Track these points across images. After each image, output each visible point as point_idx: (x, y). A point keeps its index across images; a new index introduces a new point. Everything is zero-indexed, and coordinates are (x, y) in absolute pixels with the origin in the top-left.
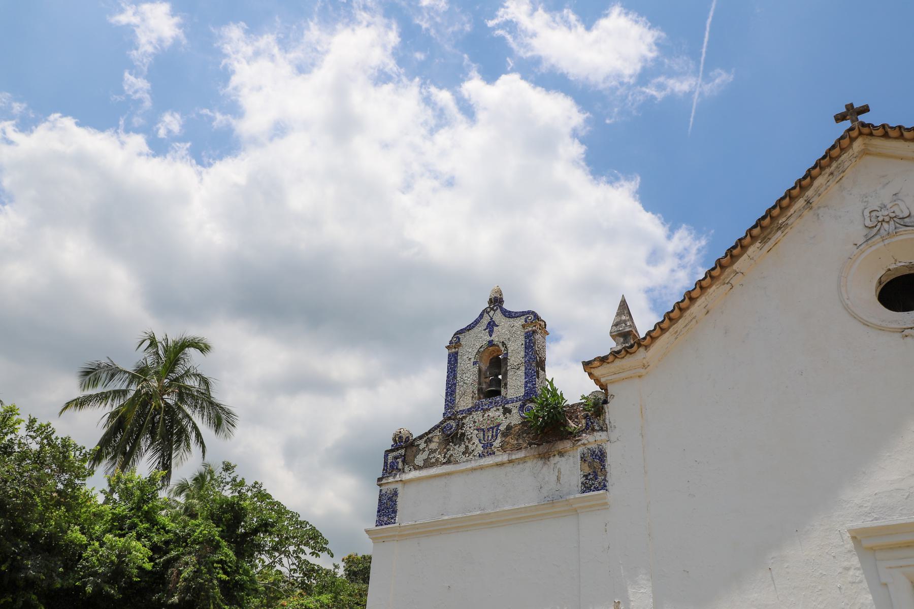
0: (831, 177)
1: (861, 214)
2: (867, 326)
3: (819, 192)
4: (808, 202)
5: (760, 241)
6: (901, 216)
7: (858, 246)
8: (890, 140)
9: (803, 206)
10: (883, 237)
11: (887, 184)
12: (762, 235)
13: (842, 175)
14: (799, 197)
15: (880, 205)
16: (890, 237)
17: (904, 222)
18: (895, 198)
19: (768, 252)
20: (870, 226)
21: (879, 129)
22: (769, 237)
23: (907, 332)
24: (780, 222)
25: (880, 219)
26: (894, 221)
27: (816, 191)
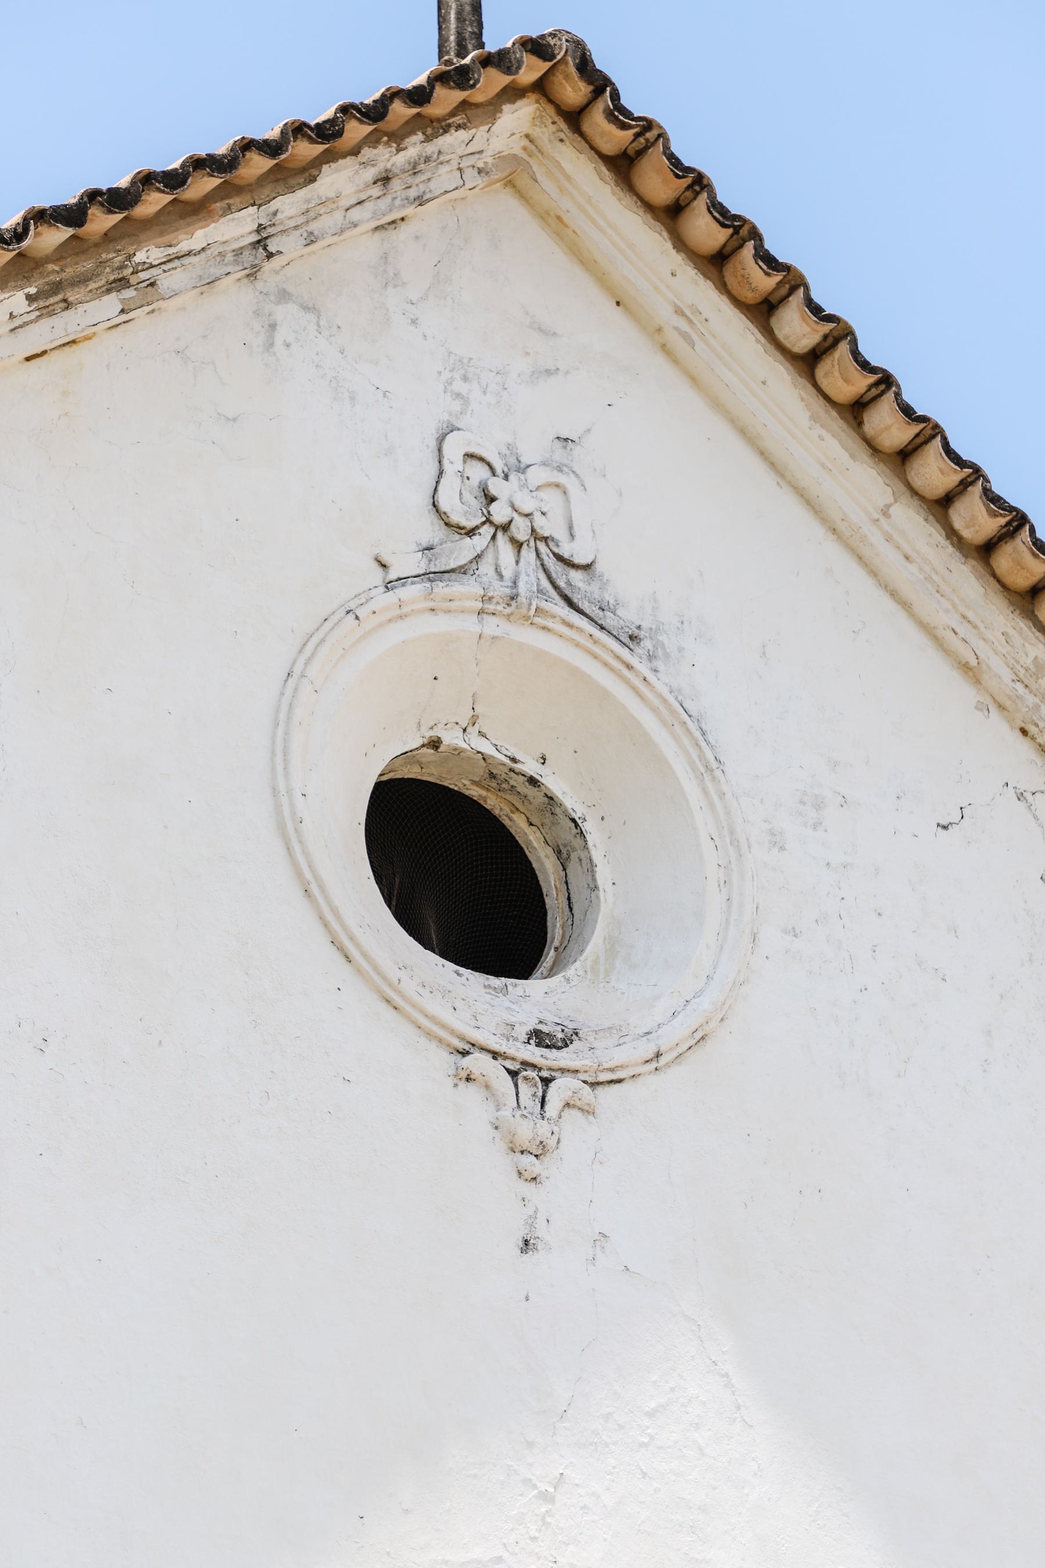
0: (376, 191)
1: (433, 444)
2: (343, 960)
3: (313, 226)
4: (259, 242)
5: (33, 290)
6: (565, 551)
7: (393, 575)
8: (629, 200)
9: (236, 245)
10: (491, 599)
11: (548, 372)
12: (51, 267)
13: (409, 211)
14: (247, 198)
15: (505, 451)
16: (508, 617)
17: (569, 583)
18: (559, 455)
19: (28, 359)
20: (455, 518)
21: (630, 127)
22: (72, 296)
23: (478, 1062)
24: (140, 257)
25: (500, 513)
26: (537, 550)
27: (309, 215)
